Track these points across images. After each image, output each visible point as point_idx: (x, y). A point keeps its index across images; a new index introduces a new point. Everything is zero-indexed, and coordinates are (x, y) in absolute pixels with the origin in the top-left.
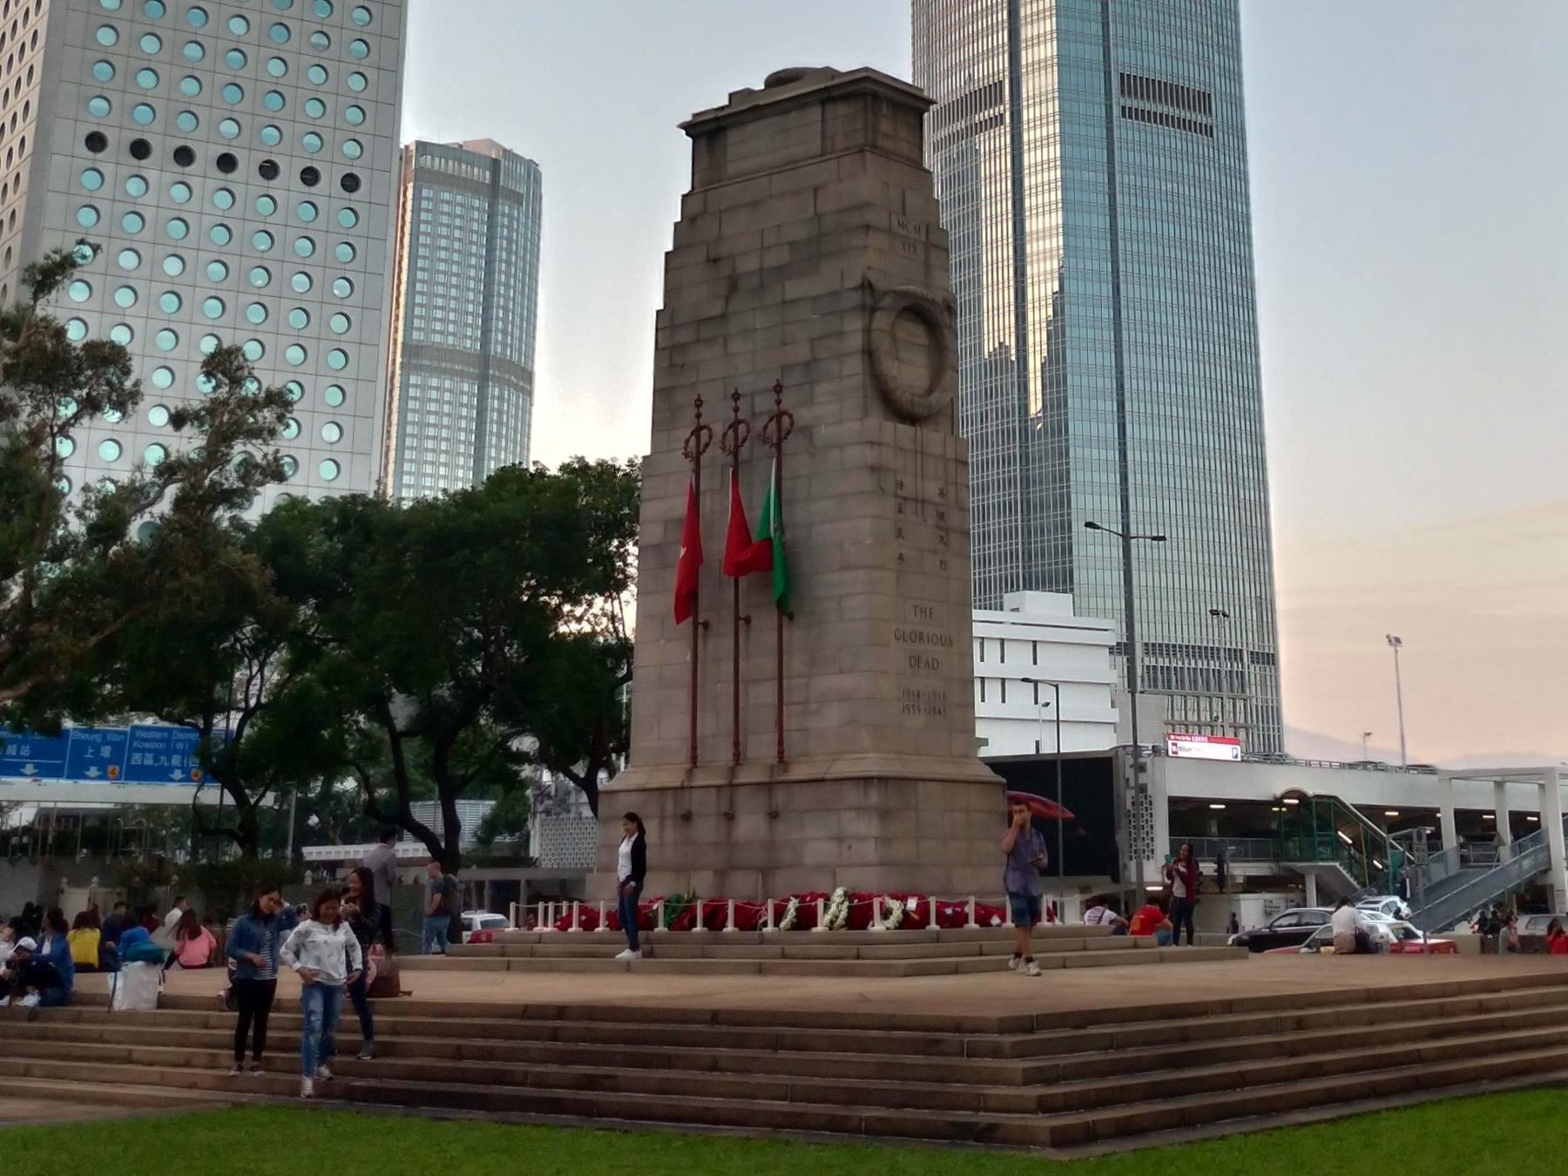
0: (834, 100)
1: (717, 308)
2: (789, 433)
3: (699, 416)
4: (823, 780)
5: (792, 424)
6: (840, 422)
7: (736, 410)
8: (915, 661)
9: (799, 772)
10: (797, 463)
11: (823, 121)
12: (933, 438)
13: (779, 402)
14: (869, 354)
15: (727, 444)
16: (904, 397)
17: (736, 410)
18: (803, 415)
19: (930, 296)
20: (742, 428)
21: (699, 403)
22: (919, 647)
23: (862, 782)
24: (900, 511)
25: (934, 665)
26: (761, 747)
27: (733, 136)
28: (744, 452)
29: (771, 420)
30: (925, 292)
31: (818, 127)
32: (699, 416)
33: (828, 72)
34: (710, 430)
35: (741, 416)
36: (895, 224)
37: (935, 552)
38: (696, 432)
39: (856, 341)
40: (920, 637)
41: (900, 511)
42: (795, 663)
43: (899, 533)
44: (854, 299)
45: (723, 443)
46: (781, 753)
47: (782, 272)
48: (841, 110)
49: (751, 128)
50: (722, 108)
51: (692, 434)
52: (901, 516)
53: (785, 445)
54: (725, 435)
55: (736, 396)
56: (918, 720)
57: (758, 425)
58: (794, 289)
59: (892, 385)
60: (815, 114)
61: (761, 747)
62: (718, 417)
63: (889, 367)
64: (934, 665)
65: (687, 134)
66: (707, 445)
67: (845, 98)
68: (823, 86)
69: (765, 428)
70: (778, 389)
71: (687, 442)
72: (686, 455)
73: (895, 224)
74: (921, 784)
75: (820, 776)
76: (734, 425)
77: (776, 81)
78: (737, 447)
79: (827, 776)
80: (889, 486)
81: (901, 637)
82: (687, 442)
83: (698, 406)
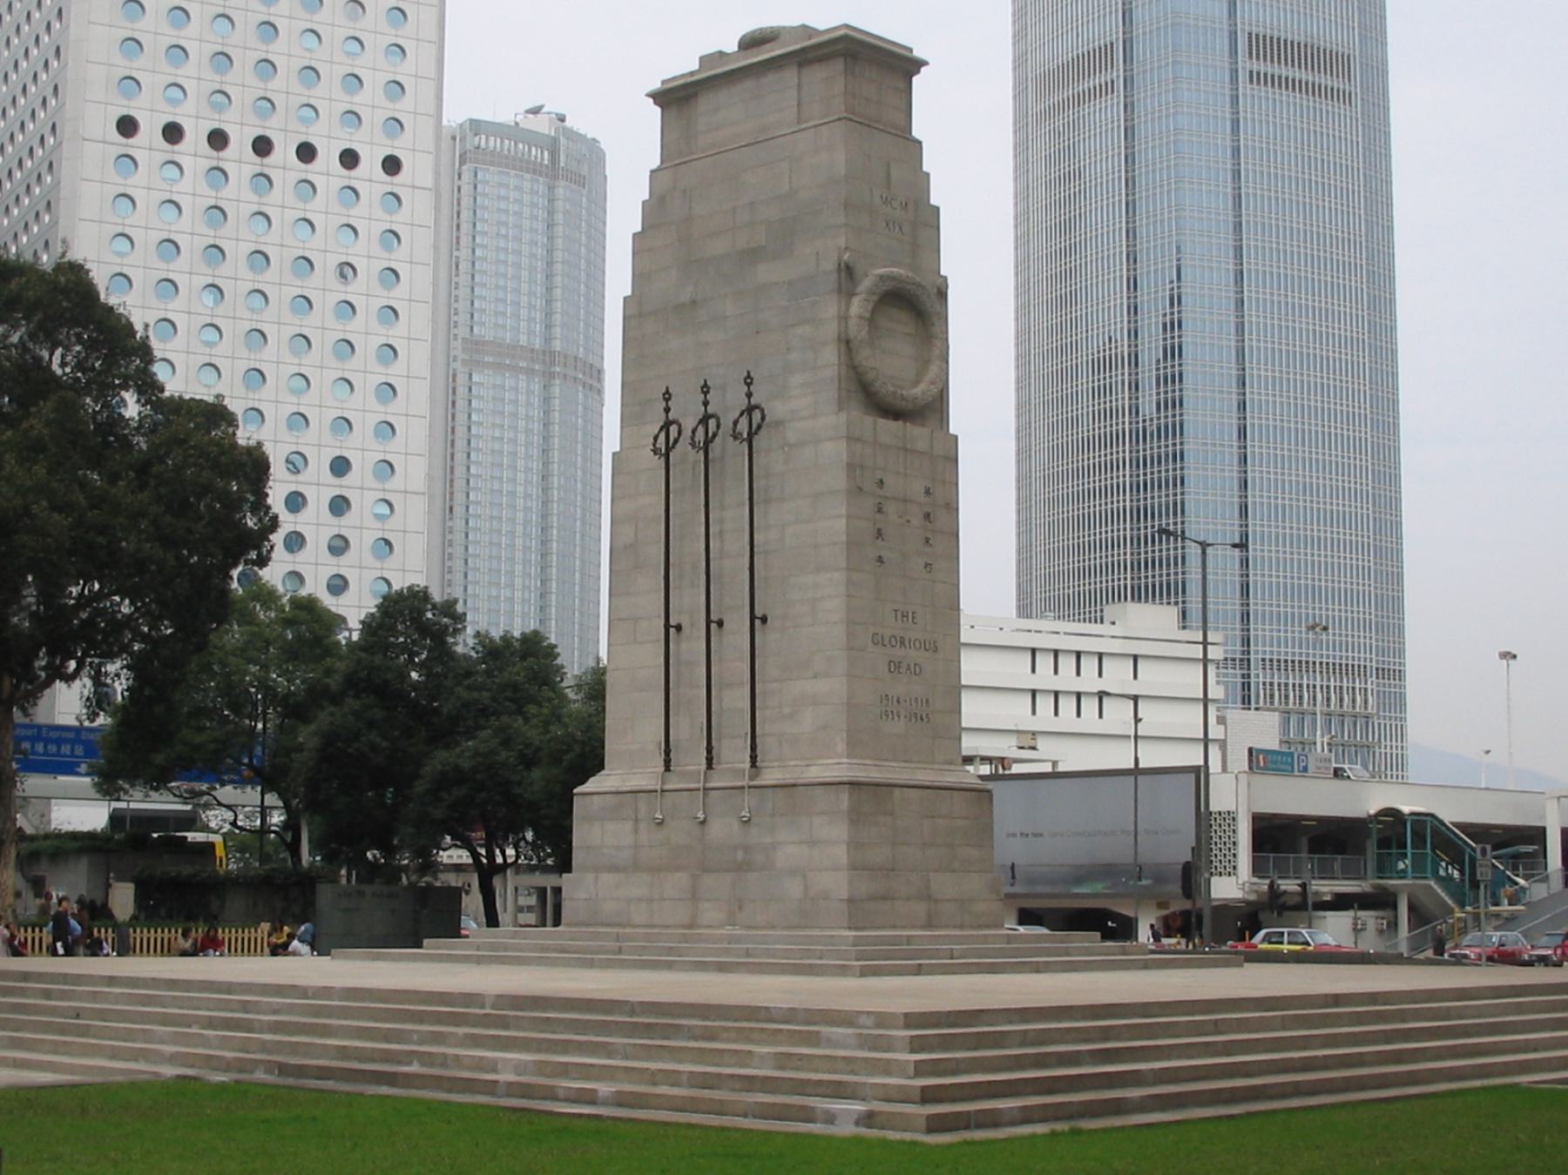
0: (811, 62)
1: (686, 295)
2: (759, 427)
3: (667, 410)
4: (794, 785)
5: (763, 418)
6: (814, 416)
7: (706, 404)
8: (895, 666)
9: (770, 776)
10: (770, 455)
11: (799, 86)
12: (918, 434)
13: (749, 395)
14: (847, 344)
15: (697, 440)
16: (885, 388)
17: (706, 404)
18: (776, 409)
19: (918, 279)
20: (712, 423)
21: (667, 396)
22: (899, 652)
23: (834, 787)
24: (880, 511)
25: (916, 670)
26: (734, 753)
27: (705, 103)
28: (715, 448)
29: (742, 414)
30: (910, 274)
31: (795, 93)
32: (667, 410)
33: (806, 30)
34: (680, 426)
35: (710, 410)
38: (666, 426)
39: (831, 330)
41: (880, 511)
42: (765, 666)
43: (879, 534)
45: (692, 439)
46: (754, 759)
47: (752, 255)
49: (723, 95)
50: (692, 73)
51: (661, 429)
52: (878, 516)
53: (756, 440)
54: (694, 431)
55: (705, 389)
56: (898, 727)
57: (727, 423)
58: (766, 272)
59: (871, 376)
60: (790, 75)
61: (734, 753)
62: (688, 412)
63: (865, 357)
64: (916, 670)
65: (655, 103)
66: (676, 441)
67: (821, 59)
68: (798, 47)
69: (736, 423)
70: (749, 380)
71: (656, 438)
72: (655, 451)
73: (877, 200)
74: (897, 791)
75: (792, 781)
76: (704, 420)
77: (751, 42)
78: (708, 442)
79: (801, 781)
81: (878, 640)
82: (656, 438)
83: (667, 400)
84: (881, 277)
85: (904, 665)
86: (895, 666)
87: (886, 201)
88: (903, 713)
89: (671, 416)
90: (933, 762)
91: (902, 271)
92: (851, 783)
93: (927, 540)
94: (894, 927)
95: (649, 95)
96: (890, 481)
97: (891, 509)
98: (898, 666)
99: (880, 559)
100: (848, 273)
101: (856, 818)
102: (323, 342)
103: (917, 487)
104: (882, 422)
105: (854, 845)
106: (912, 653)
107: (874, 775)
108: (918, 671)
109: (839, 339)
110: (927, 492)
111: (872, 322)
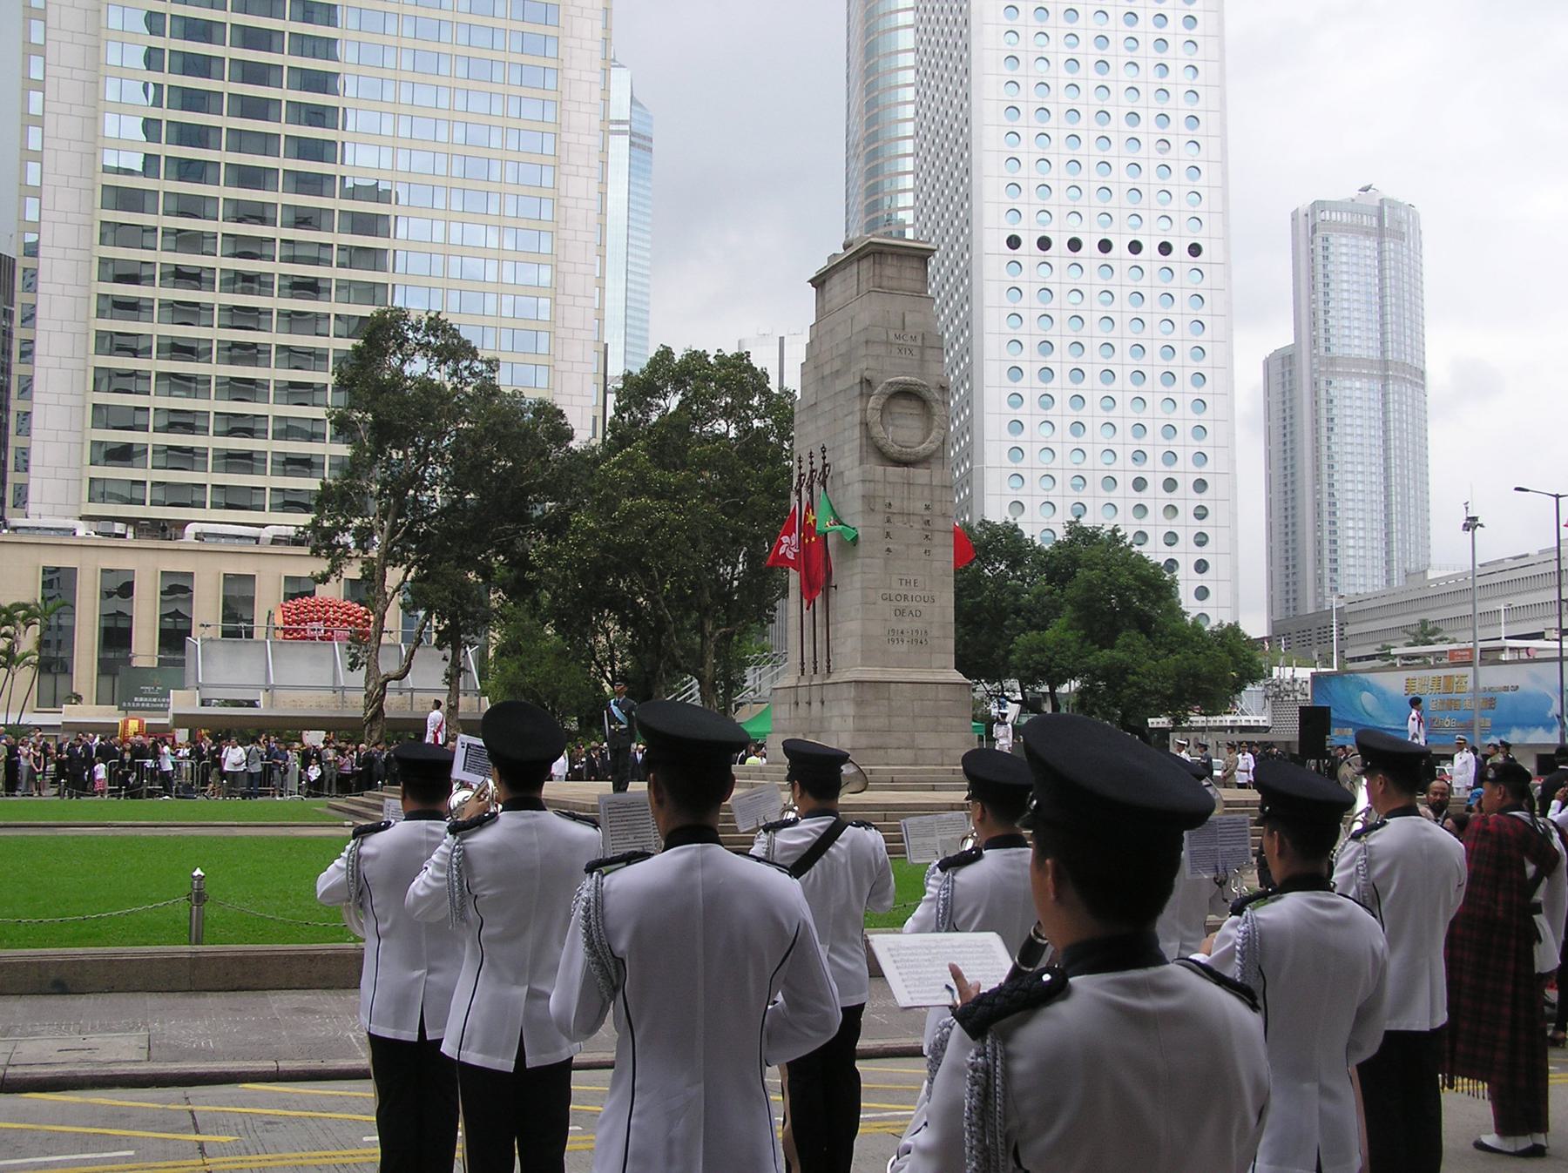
14: (865, 425)
16: (894, 450)
22: (903, 604)
25: (918, 614)
35: (814, 467)
36: (892, 336)
37: (920, 545)
39: (857, 418)
40: (906, 597)
44: (857, 390)
48: (865, 264)
56: (904, 647)
59: (882, 443)
63: (877, 431)
64: (918, 614)
73: (892, 336)
74: (893, 685)
80: (879, 506)
84: (890, 383)
85: (907, 611)
86: (901, 612)
87: (899, 338)
88: (906, 640)
89: (814, 467)
90: (931, 668)
91: (913, 379)
92: (855, 682)
93: (927, 536)
94: (887, 764)
95: (810, 281)
96: (896, 504)
97: (895, 519)
98: (902, 613)
99: (888, 550)
100: (867, 383)
101: (860, 703)
102: (1154, 375)
103: (919, 506)
104: (891, 469)
105: (858, 717)
106: (914, 603)
107: (878, 676)
108: (918, 614)
109: (861, 423)
110: (927, 508)
111: (884, 410)
